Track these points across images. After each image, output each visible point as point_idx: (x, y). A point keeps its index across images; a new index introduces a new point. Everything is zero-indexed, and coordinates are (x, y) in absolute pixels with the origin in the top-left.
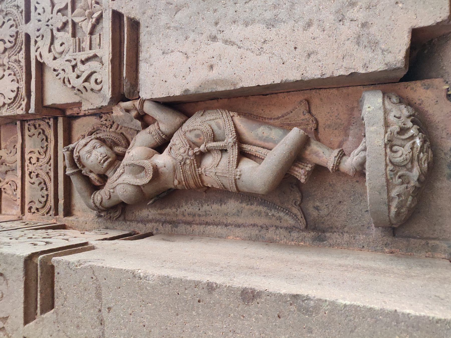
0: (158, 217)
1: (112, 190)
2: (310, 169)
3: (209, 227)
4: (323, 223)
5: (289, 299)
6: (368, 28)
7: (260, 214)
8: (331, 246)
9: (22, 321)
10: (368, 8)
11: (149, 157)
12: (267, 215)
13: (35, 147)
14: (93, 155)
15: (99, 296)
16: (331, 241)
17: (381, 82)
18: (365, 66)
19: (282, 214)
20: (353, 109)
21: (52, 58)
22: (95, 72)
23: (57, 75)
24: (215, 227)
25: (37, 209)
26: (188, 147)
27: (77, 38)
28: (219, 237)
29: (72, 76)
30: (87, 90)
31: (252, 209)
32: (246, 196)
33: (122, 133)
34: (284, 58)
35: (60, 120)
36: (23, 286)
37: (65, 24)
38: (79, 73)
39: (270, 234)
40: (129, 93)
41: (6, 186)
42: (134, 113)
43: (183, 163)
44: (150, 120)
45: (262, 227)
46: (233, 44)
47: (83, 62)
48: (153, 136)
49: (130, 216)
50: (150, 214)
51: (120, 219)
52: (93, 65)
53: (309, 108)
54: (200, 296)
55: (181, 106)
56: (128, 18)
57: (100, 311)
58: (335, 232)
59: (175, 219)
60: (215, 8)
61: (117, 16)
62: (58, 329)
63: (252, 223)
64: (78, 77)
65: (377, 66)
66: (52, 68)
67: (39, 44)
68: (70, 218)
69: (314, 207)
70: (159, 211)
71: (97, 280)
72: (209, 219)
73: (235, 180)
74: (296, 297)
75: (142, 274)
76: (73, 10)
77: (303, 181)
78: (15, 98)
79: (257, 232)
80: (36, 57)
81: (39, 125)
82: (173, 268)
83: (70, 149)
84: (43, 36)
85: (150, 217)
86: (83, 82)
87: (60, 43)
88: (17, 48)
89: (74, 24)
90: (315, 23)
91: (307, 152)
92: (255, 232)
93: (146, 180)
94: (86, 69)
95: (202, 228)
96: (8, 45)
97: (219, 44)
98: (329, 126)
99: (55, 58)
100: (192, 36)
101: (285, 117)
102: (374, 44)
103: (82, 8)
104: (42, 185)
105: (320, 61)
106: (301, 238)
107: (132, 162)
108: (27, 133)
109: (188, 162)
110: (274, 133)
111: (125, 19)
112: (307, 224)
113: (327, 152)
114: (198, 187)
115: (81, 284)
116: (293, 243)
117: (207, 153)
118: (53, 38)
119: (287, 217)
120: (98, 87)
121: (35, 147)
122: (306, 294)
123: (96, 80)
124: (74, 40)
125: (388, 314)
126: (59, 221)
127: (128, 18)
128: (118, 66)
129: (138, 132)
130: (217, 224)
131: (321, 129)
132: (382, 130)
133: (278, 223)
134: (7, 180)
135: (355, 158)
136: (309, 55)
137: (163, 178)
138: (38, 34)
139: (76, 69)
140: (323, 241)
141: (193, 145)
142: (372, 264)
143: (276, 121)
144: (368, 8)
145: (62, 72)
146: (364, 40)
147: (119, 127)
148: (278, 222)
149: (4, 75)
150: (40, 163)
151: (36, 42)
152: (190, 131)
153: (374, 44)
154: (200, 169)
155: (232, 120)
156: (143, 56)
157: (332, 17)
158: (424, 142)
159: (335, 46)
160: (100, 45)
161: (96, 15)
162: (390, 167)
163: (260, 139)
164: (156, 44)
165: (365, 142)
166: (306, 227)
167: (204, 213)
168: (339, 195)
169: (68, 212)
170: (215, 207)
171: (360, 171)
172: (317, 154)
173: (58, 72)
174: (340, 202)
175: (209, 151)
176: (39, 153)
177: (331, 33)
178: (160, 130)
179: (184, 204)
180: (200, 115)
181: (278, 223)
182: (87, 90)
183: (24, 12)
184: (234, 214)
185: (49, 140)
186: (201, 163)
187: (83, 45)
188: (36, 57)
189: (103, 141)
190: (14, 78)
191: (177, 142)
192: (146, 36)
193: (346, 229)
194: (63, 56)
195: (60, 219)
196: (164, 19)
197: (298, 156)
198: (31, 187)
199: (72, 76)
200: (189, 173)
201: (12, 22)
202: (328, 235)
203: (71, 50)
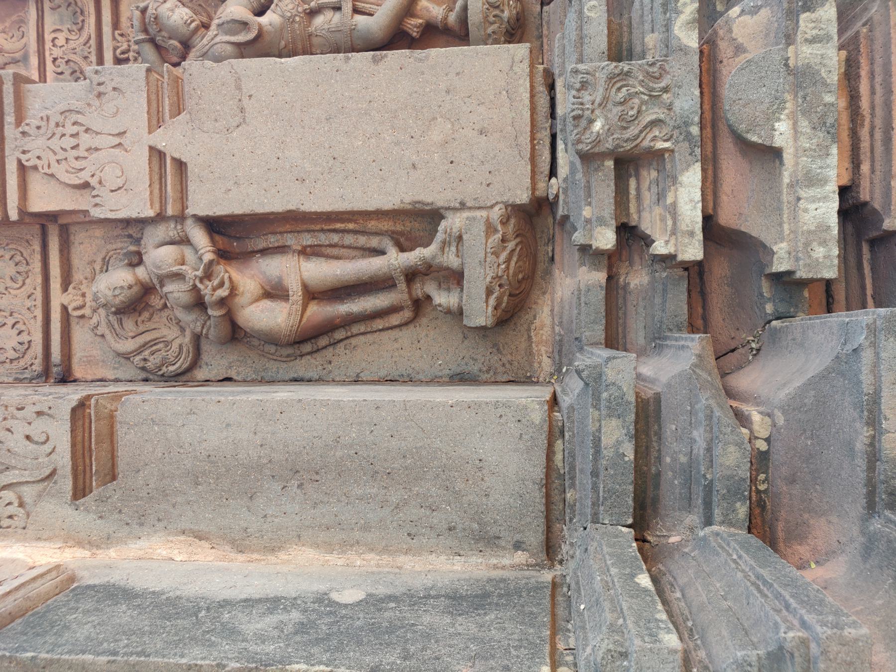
9: (147, 130)
15: (239, 88)
33: (200, 5)
36: (146, 96)
43: (291, 20)
57: (240, 100)
71: (236, 73)
77: (415, 34)
91: (419, 8)
93: (251, 36)
104: (78, 74)
109: (297, 19)
113: (436, 7)
137: (267, 38)
150: (72, 44)
176: (69, 31)
185: (86, 13)
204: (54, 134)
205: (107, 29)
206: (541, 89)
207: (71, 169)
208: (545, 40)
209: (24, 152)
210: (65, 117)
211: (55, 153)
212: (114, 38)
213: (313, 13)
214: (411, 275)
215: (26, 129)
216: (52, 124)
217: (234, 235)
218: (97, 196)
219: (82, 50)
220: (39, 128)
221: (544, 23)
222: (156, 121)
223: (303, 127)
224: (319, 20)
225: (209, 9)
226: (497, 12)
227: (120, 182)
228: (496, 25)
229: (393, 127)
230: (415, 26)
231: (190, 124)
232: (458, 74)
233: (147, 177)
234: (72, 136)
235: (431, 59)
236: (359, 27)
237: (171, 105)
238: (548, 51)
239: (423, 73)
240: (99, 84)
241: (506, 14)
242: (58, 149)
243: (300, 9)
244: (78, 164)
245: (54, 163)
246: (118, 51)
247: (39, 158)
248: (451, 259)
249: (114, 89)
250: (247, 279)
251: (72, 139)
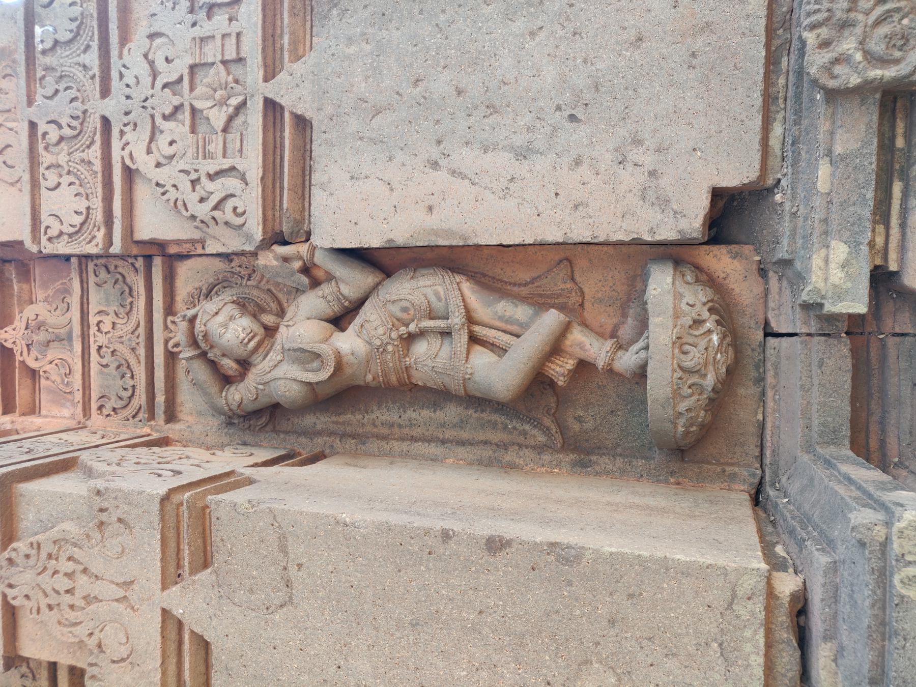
0: (333, 427)
1: (261, 387)
2: (571, 368)
3: (416, 444)
4: (587, 441)
5: (545, 548)
6: (657, 179)
7: (494, 425)
8: (597, 474)
9: (159, 585)
10: (658, 151)
11: (326, 340)
12: (505, 427)
13: (108, 305)
14: (231, 328)
15: (284, 550)
16: (597, 468)
18: (652, 231)
19: (527, 427)
20: (634, 278)
21: (154, 164)
22: (232, 196)
23: (163, 194)
24: (426, 444)
25: (114, 409)
26: (390, 326)
27: (200, 135)
28: (432, 460)
29: (192, 198)
30: (217, 223)
31: (483, 418)
32: (477, 401)
33: (269, 290)
34: (540, 208)
35: (158, 262)
36: (159, 536)
37: (177, 109)
38: (204, 194)
39: (510, 456)
40: (292, 233)
41: (47, 368)
42: (297, 265)
43: (381, 350)
44: (320, 274)
45: (498, 446)
46: (464, 177)
47: (211, 177)
48: (329, 302)
49: (284, 425)
50: (318, 422)
51: (268, 429)
52: (231, 184)
53: (572, 272)
54: (431, 546)
56: (292, 113)
57: (285, 568)
58: (604, 454)
59: (360, 430)
60: (436, 117)
61: (272, 108)
62: (219, 595)
63: (483, 438)
64: (202, 200)
65: (667, 234)
66: (154, 182)
67: (128, 137)
68: (177, 426)
69: (575, 418)
70: (334, 418)
71: (280, 527)
72: (416, 432)
73: (464, 379)
74: (553, 545)
75: (348, 519)
76: (192, 89)
77: (560, 383)
78: (82, 224)
79: (491, 452)
80: (123, 158)
81: (116, 267)
82: (386, 510)
83: (187, 318)
84: (135, 125)
85: (319, 427)
86: (212, 210)
87: (169, 140)
88: (85, 139)
89: (194, 110)
90: (586, 162)
91: (567, 343)
92: (487, 453)
93: (324, 375)
94: (218, 188)
95: (405, 446)
96: (67, 132)
97: (442, 175)
98: (600, 301)
99: (158, 165)
100: (400, 156)
101: (536, 284)
102: (663, 203)
103: (209, 86)
104: (124, 369)
105: (590, 217)
106: (554, 463)
107: (300, 346)
108: (92, 279)
109: (390, 348)
110: (521, 312)
111: (287, 115)
112: (564, 443)
114: (401, 384)
115: (255, 534)
116: (543, 470)
117: (418, 335)
118: (155, 131)
119: (535, 432)
120: (239, 221)
121: (108, 305)
122: (566, 542)
123: (235, 209)
124: (195, 138)
125: (657, 560)
126: (157, 431)
127: (292, 113)
128: (271, 186)
129: (299, 291)
130: (429, 440)
131: (587, 305)
132: (670, 323)
133: (521, 439)
134: (49, 357)
135: (634, 357)
136: (576, 207)
137: (348, 371)
138: (126, 119)
139: (198, 187)
140: (587, 467)
141: (396, 323)
142: (651, 501)
143: (523, 288)
144: (658, 151)
145: (172, 189)
146: (651, 195)
147: (265, 280)
148: (522, 438)
149: (59, 184)
151: (122, 133)
152: (394, 302)
153: (663, 203)
154: (407, 359)
155: (460, 290)
156: (316, 178)
157: (608, 156)
158: (723, 338)
159: (613, 198)
160: (241, 151)
161: (234, 101)
162: (679, 374)
163: (501, 318)
164: (339, 162)
165: (647, 338)
166: (563, 446)
167: (407, 423)
168: (610, 401)
169: (171, 416)
170: (426, 413)
171: (641, 374)
172: (581, 346)
173: (165, 189)
174: (612, 412)
175: (422, 334)
176: (116, 314)
177: (607, 178)
178: (341, 294)
179: (375, 408)
180: (409, 277)
181: (521, 439)
182: (217, 223)
183: (97, 79)
184: (455, 426)
185: (135, 293)
186: (408, 350)
187: (211, 148)
188: (123, 158)
189: (242, 305)
190: (81, 190)
191: (373, 317)
192: (323, 147)
193: (619, 450)
194: (174, 162)
195: (157, 427)
196: (353, 124)
197: (555, 349)
198: (101, 373)
199: (192, 198)
200: (391, 365)
201: (73, 93)
202: (594, 458)
203: (189, 155)
204: (45, 569)
205: (158, 316)
206: (786, 635)
207: (64, 621)
208: (770, 393)
209: (11, 586)
210: (60, 548)
211: (46, 595)
212: (166, 327)
213: (411, 338)
215: (13, 555)
216: (43, 555)
218: (95, 665)
219: (130, 340)
220: (27, 556)
221: (769, 365)
222: (171, 575)
223: (376, 629)
224: (421, 348)
225: (280, 296)
226: (695, 379)
227: (124, 651)
228: (696, 397)
229: (517, 660)
230: (563, 375)
231: (216, 587)
232: (631, 596)
233: (158, 653)
234: (66, 574)
235: (584, 563)
236: (477, 378)
237: (192, 554)
238: (774, 411)
239: (570, 583)
240: (101, 510)
241: (710, 381)
242: (49, 590)
243: (394, 335)
244: (72, 616)
245: (44, 609)
246: (171, 344)
247: (27, 596)
249: (120, 520)
251: (66, 580)
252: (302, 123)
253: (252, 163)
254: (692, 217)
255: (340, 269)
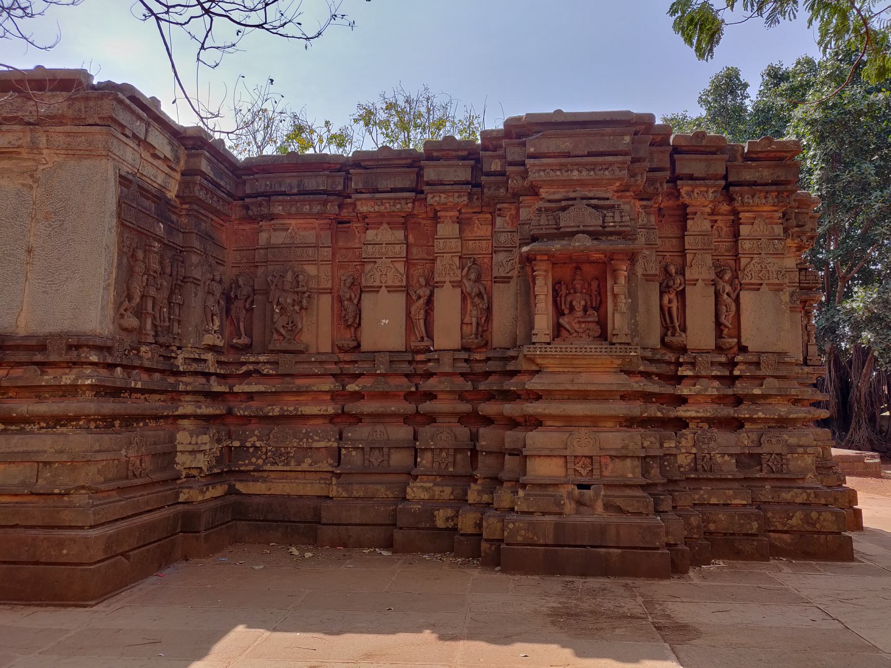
17: (739, 342)
55: (737, 301)
61: (761, 284)
94: (749, 275)
197: (726, 326)
214: (674, 327)
217: (682, 294)
248: (677, 334)
250: (672, 296)
252: (759, 289)
253: (753, 281)
254: (744, 344)
255: (736, 294)
